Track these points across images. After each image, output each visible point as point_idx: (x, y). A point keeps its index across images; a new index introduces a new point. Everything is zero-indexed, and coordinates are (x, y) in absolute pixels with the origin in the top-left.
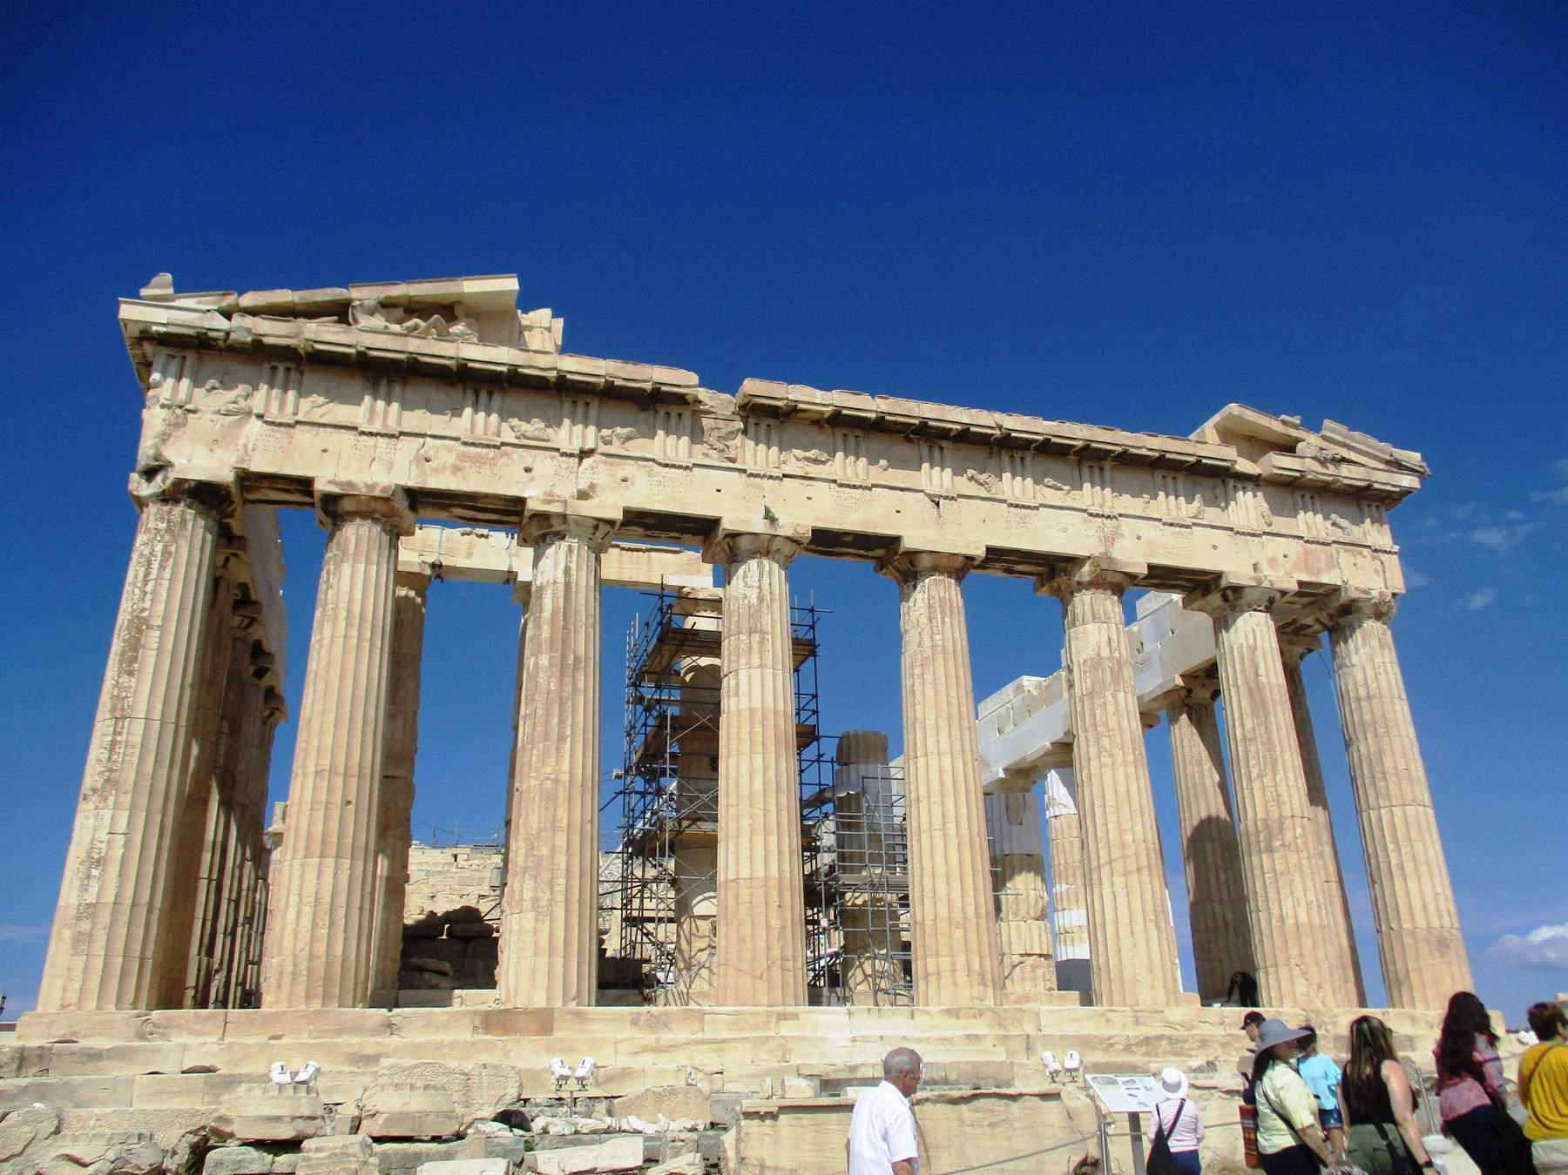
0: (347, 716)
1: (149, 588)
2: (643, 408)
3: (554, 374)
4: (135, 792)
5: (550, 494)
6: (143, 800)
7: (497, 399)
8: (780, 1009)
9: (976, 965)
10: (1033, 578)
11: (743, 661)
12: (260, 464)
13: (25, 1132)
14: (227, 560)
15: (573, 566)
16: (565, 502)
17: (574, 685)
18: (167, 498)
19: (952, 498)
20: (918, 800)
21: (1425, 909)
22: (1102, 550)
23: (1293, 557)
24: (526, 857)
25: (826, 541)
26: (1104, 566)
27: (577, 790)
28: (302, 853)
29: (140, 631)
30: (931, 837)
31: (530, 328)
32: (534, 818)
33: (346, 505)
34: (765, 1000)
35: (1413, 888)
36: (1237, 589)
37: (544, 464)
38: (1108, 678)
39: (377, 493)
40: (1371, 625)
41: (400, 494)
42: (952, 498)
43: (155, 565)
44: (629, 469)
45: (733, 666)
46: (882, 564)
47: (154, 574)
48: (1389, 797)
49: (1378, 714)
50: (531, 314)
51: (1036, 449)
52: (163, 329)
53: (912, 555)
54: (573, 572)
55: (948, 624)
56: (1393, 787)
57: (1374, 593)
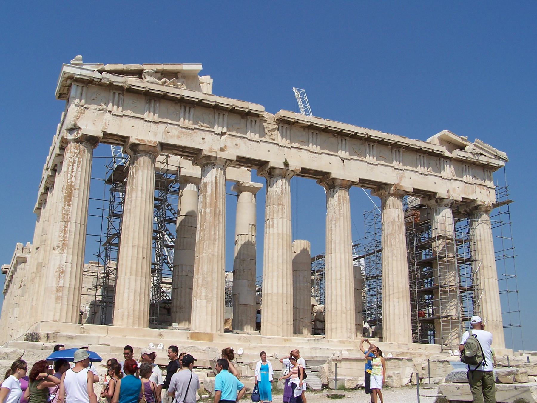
0: (143, 227)
1: (74, 174)
2: (243, 118)
3: (214, 103)
4: (73, 248)
6: (76, 252)
8: (286, 337)
9: (349, 327)
10: (371, 190)
11: (275, 215)
12: (111, 130)
15: (218, 176)
16: (216, 152)
17: (219, 220)
18: (77, 141)
19: (349, 159)
20: (331, 269)
21: (492, 314)
22: (398, 182)
24: (203, 280)
25: (305, 172)
26: (398, 188)
27: (220, 258)
28: (128, 274)
29: (71, 190)
30: (336, 282)
31: (203, 83)
33: (141, 148)
34: (281, 334)
35: (489, 307)
36: (442, 199)
37: (209, 137)
39: (152, 145)
40: (485, 217)
41: (159, 145)
42: (349, 159)
43: (75, 165)
44: (238, 141)
45: (271, 217)
46: (320, 181)
47: (75, 169)
48: (484, 275)
49: (483, 247)
50: (203, 77)
51: (378, 142)
52: (78, 77)
53: (334, 179)
54: (218, 178)
55: (345, 206)
56: (486, 273)
57: (486, 203)
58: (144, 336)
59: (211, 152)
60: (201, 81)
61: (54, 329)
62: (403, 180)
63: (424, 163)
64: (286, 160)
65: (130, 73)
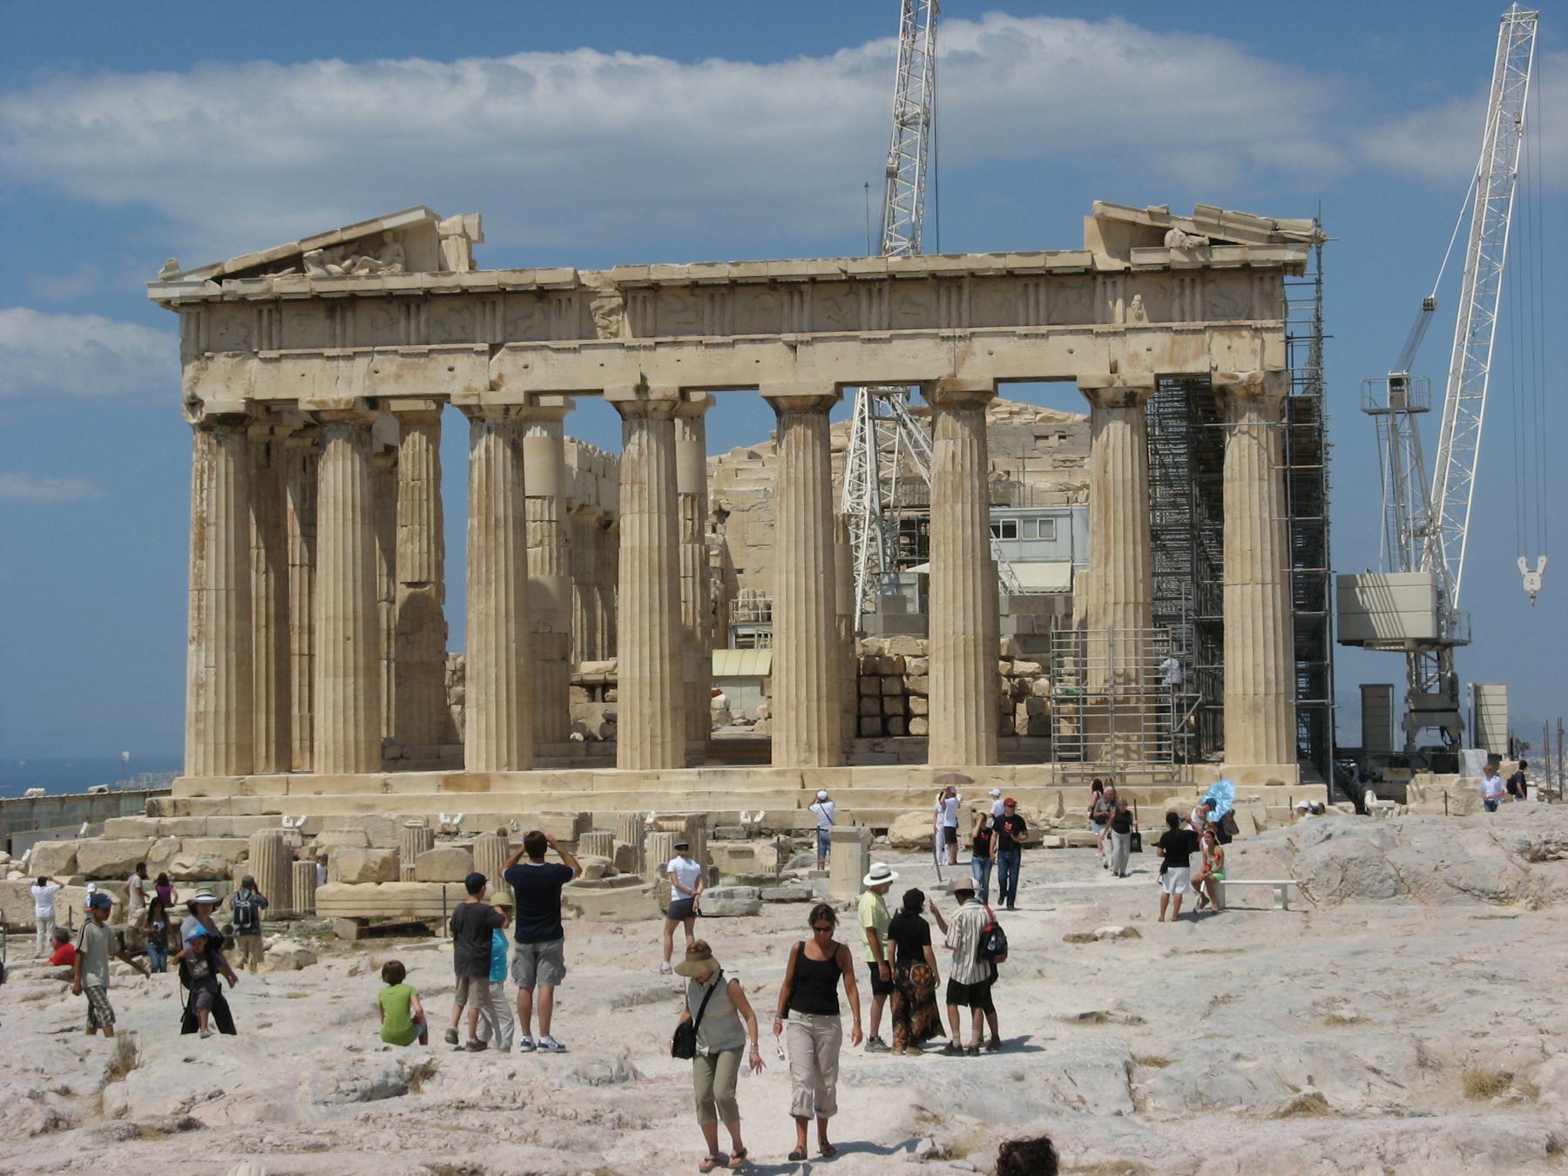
5: (468, 389)
6: (223, 644)
7: (424, 309)
12: (265, 391)
13: (165, 851)
14: (272, 431)
18: (205, 427)
22: (950, 371)
23: (1157, 350)
26: (949, 388)
27: (502, 621)
32: (475, 642)
33: (324, 416)
38: (949, 492)
43: (205, 477)
44: (529, 357)
58: (355, 789)
59: (466, 397)
60: (442, 232)
61: (195, 790)
62: (967, 363)
63: (1037, 303)
64: (643, 378)
65: (276, 266)
